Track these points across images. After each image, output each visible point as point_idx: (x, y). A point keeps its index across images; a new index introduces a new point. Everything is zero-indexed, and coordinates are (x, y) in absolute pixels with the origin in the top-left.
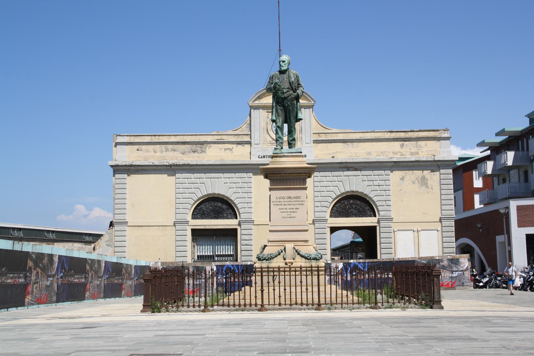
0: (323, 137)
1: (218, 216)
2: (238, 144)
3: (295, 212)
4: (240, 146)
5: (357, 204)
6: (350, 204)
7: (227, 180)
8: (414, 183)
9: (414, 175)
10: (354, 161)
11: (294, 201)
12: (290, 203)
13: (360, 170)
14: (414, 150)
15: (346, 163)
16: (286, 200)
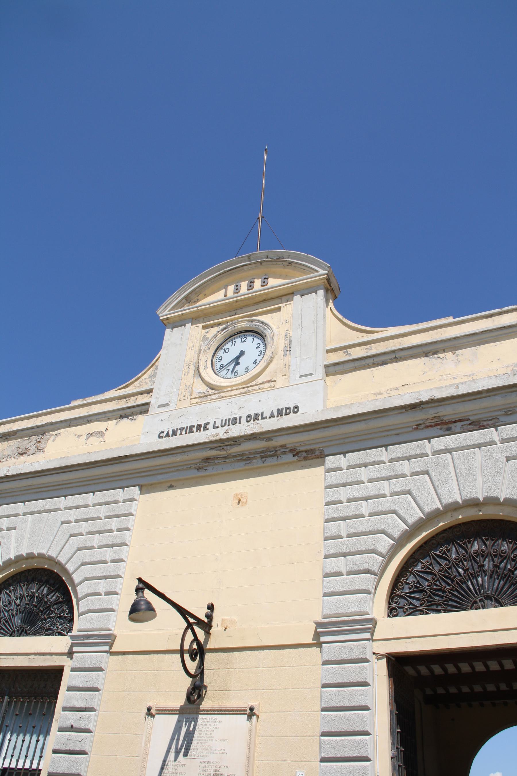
0: (358, 353)
1: (32, 623)
2: (122, 417)
4: (125, 420)
5: (503, 556)
6: (473, 558)
7: (72, 515)
10: (462, 391)
13: (494, 423)
15: (433, 402)
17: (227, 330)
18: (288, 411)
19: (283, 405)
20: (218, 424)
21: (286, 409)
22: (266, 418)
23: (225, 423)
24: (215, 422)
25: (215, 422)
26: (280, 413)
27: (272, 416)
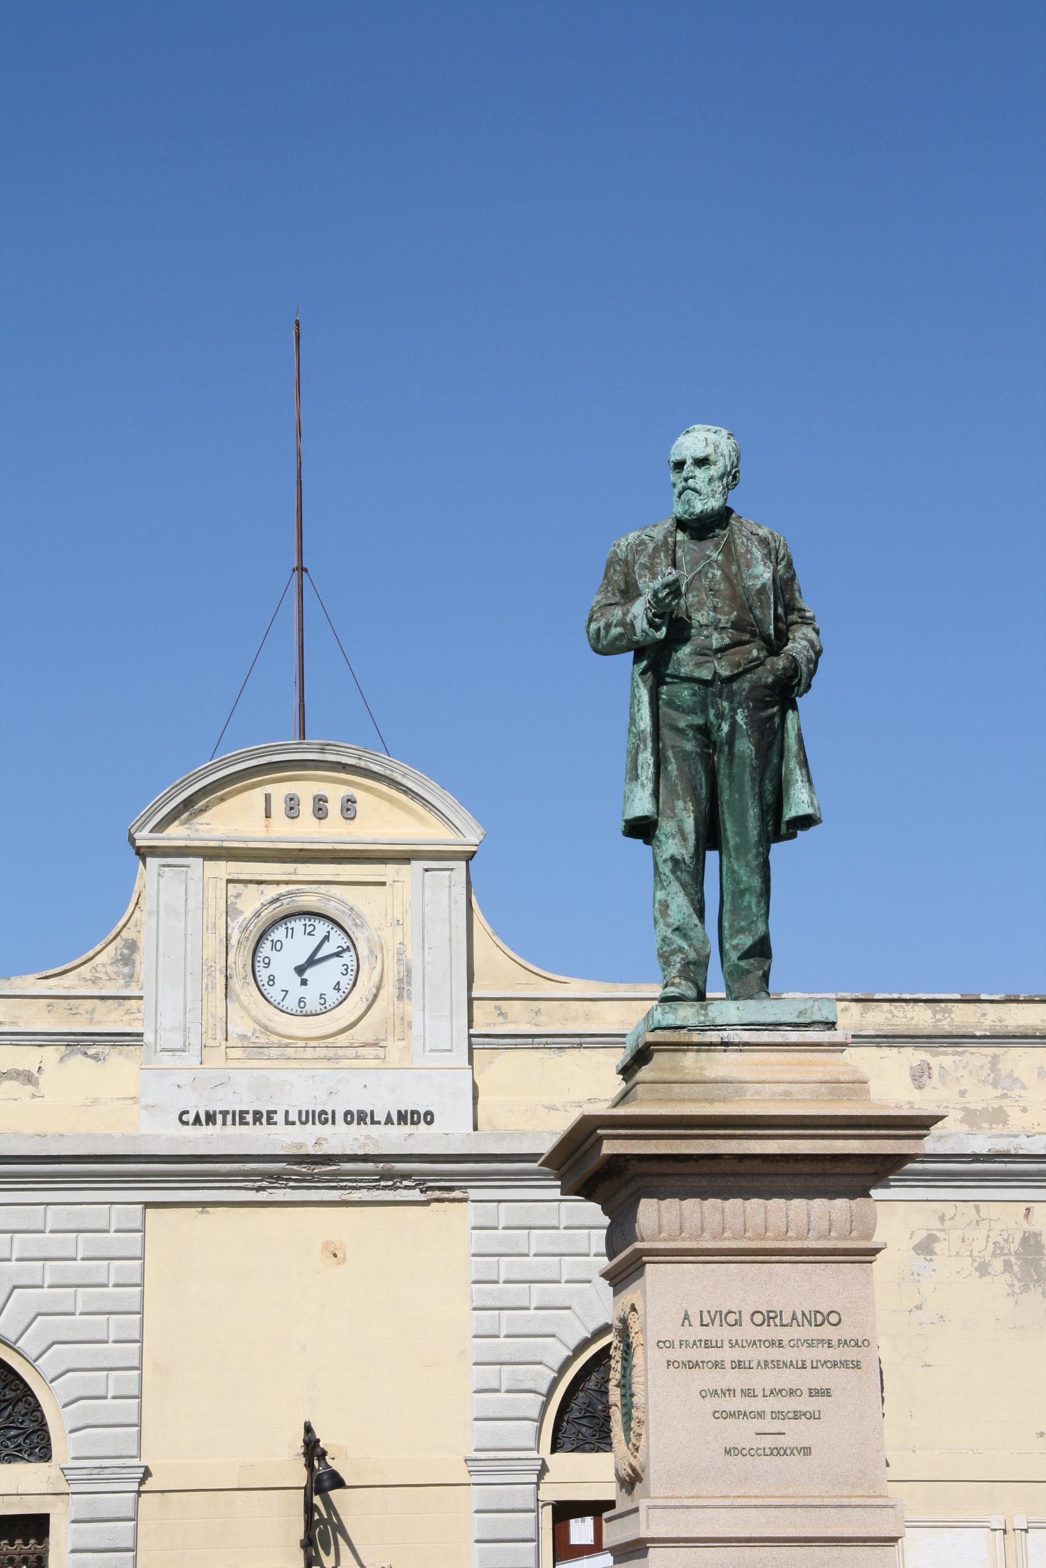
3: (812, 1416)
8: (983, 1269)
9: (984, 1226)
11: (795, 1344)
12: (774, 1354)
14: (982, 1097)
16: (748, 1331)
17: (279, 904)
18: (415, 1119)
19: (407, 1106)
20: (293, 1117)
21: (413, 1112)
22: (379, 1123)
23: (308, 1118)
24: (287, 1112)
25: (287, 1112)
26: (402, 1118)
27: (389, 1121)
